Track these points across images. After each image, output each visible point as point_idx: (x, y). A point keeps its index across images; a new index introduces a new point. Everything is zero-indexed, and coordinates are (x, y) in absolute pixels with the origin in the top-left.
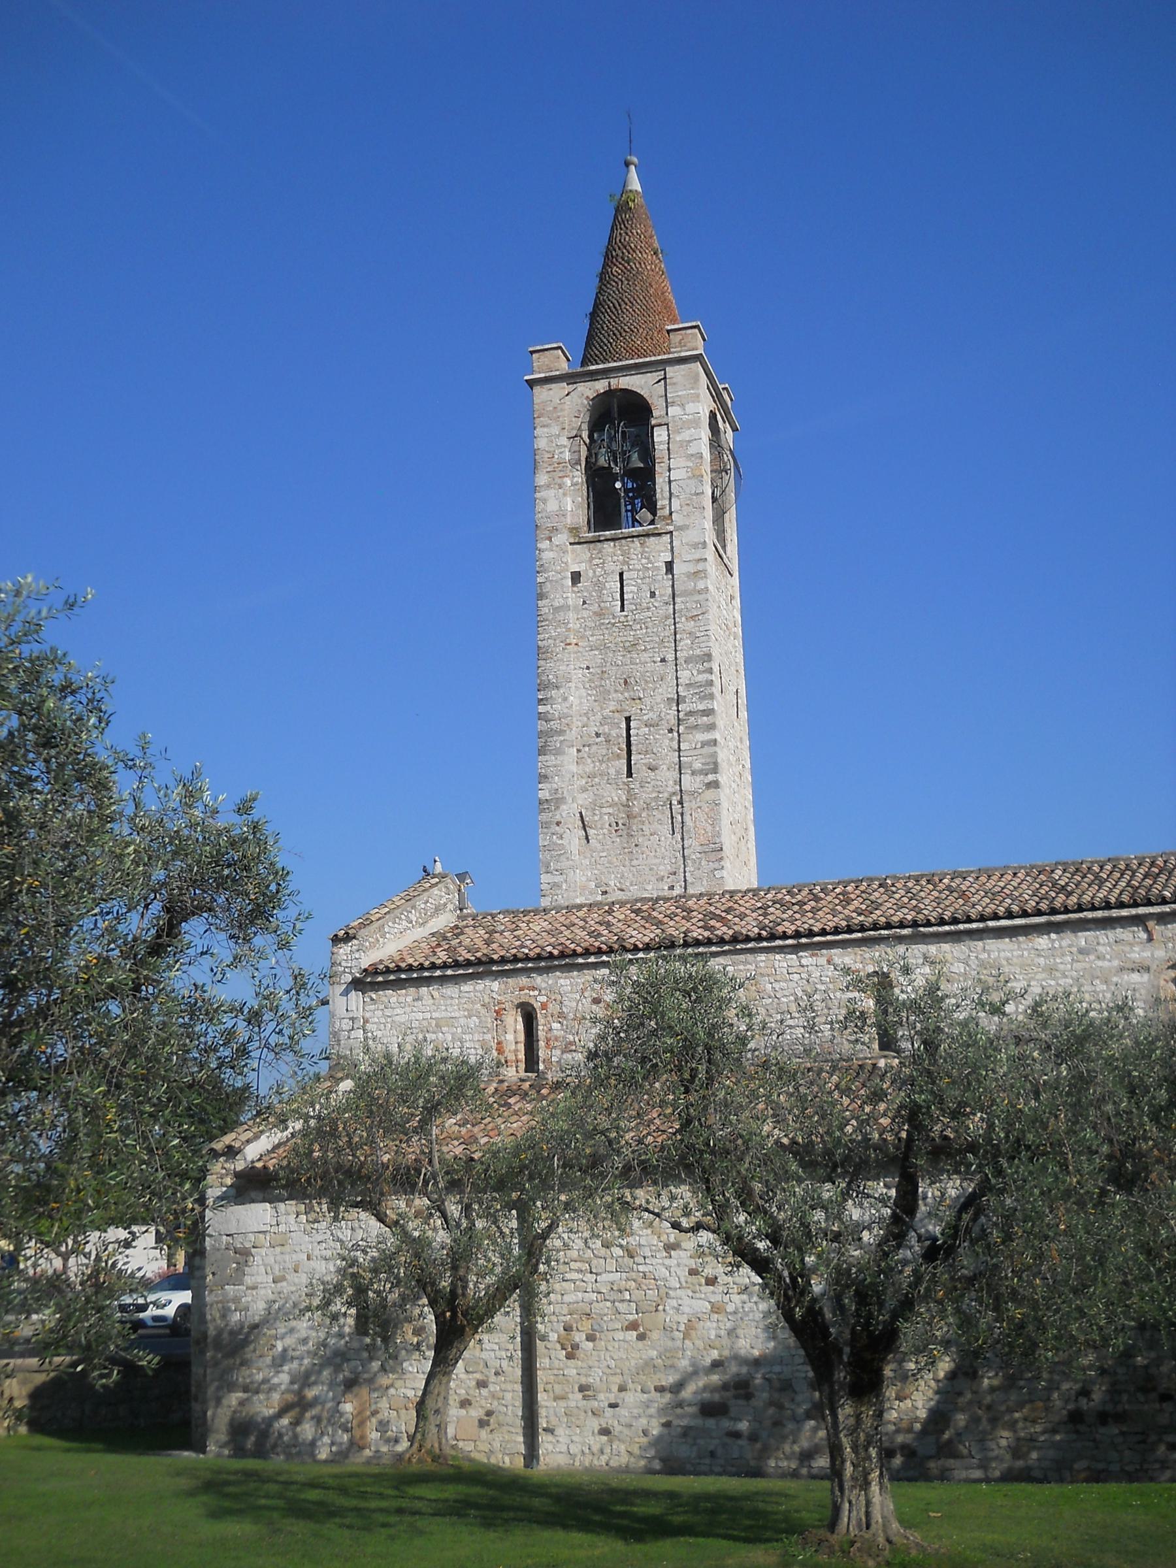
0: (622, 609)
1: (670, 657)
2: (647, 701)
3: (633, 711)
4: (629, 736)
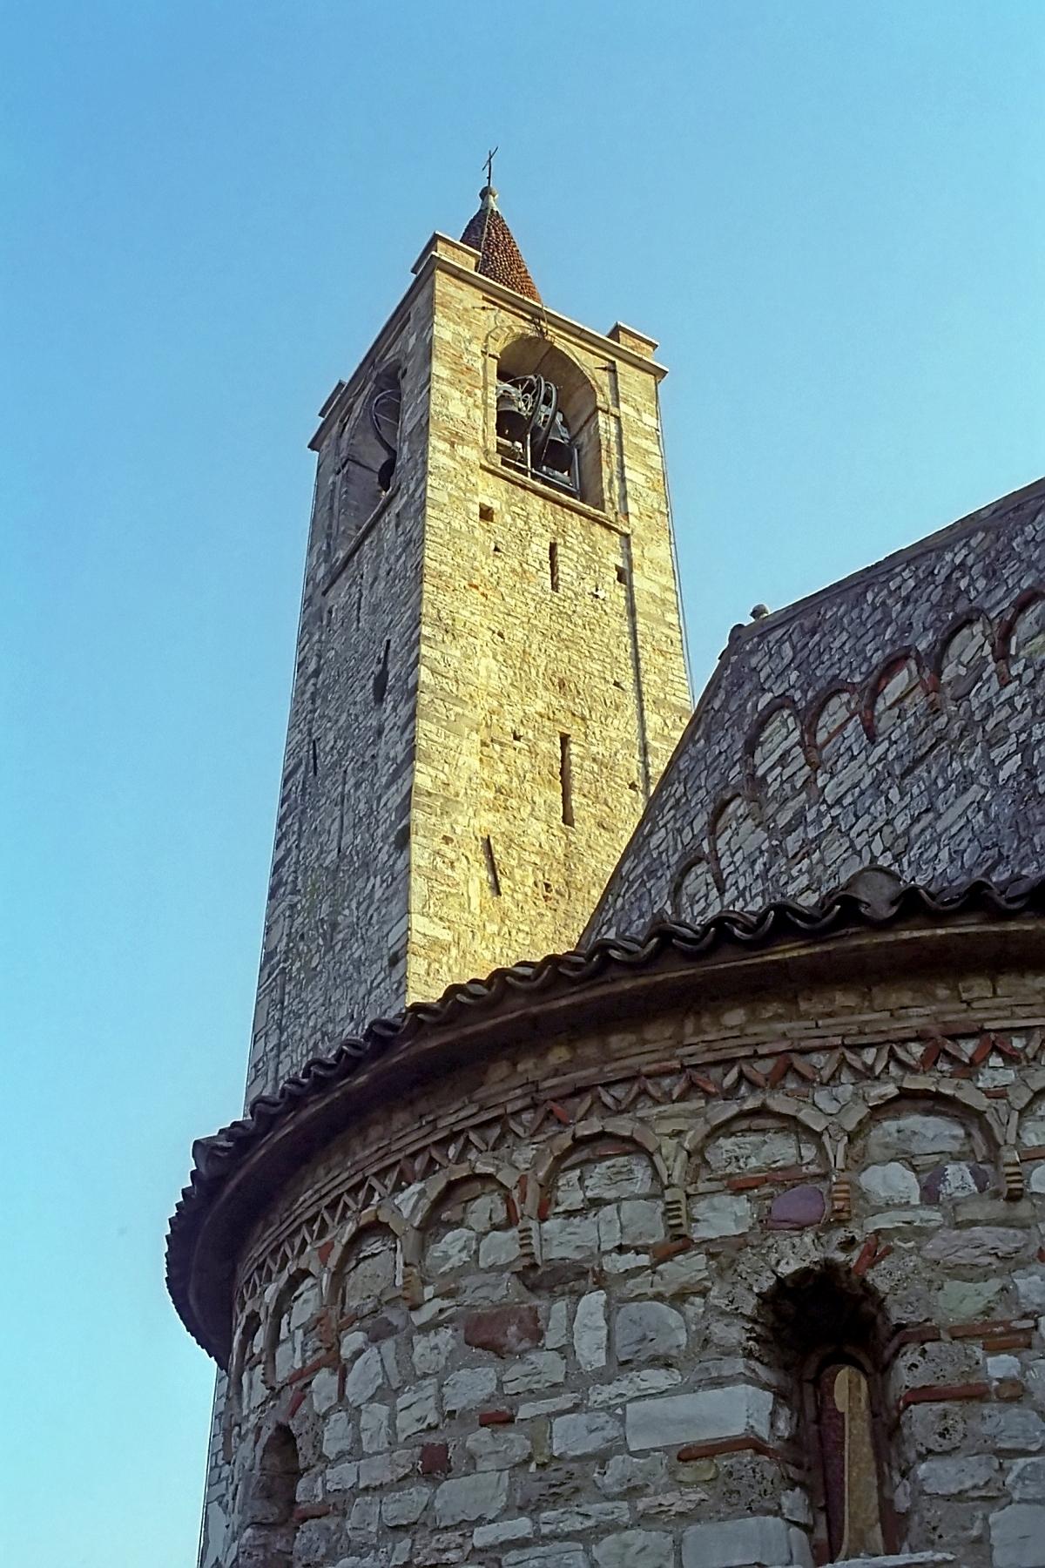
0: (555, 587)
1: (628, 684)
2: (595, 727)
3: (574, 730)
4: (564, 759)
